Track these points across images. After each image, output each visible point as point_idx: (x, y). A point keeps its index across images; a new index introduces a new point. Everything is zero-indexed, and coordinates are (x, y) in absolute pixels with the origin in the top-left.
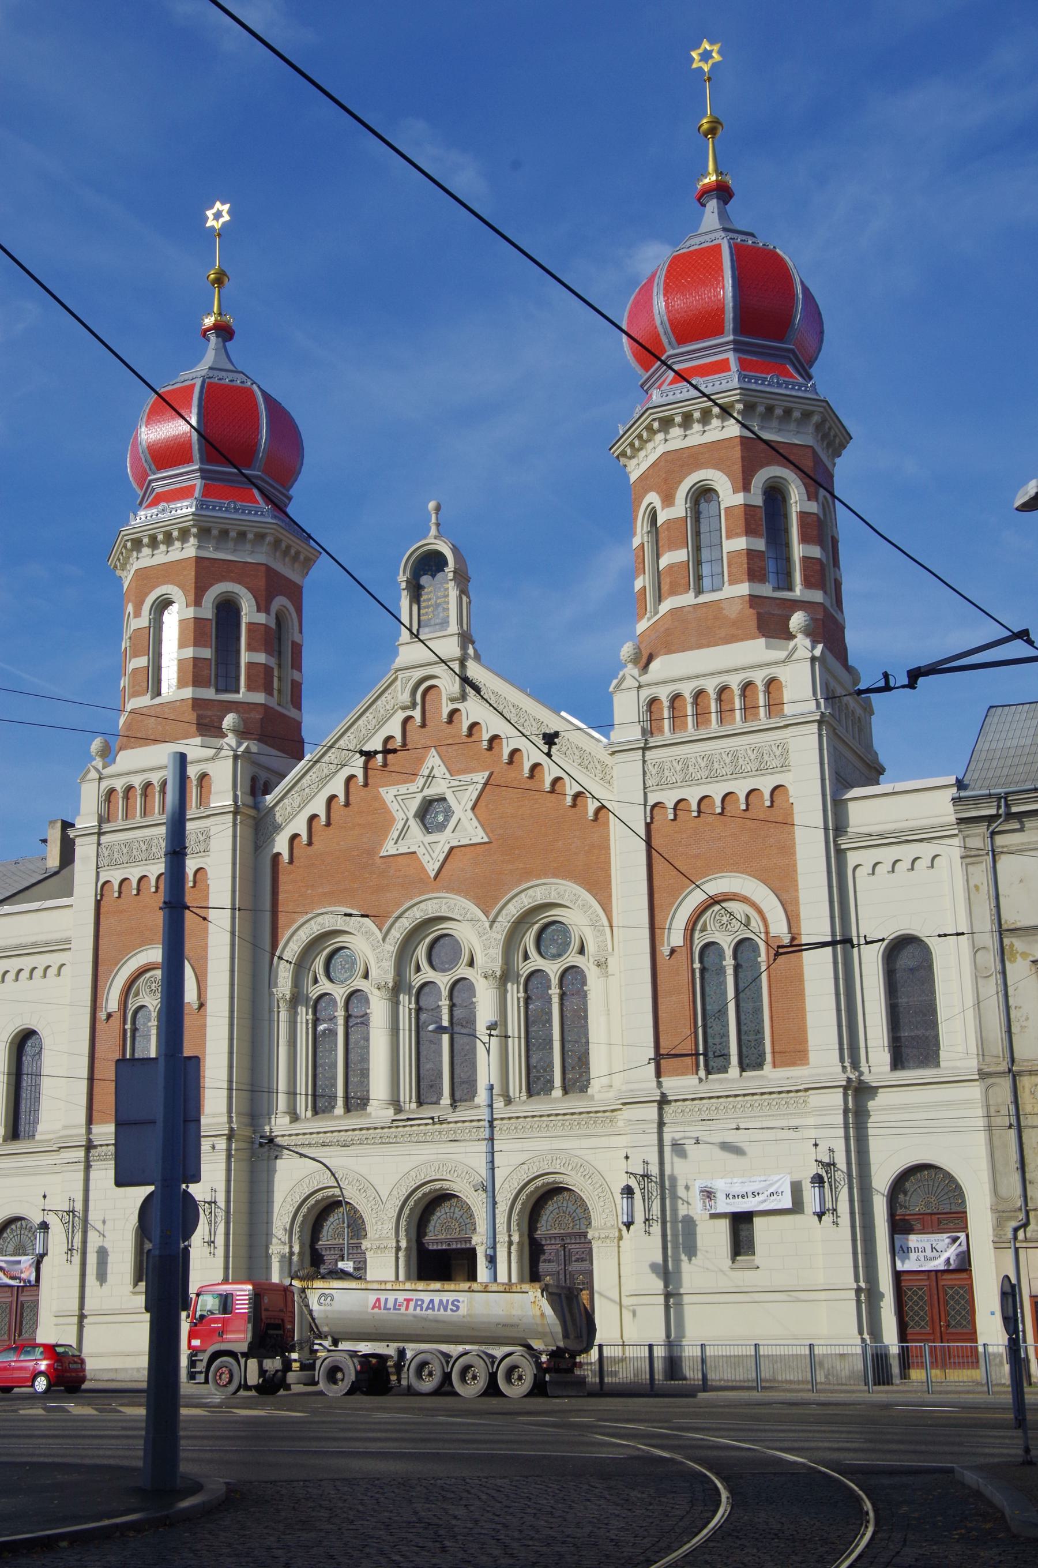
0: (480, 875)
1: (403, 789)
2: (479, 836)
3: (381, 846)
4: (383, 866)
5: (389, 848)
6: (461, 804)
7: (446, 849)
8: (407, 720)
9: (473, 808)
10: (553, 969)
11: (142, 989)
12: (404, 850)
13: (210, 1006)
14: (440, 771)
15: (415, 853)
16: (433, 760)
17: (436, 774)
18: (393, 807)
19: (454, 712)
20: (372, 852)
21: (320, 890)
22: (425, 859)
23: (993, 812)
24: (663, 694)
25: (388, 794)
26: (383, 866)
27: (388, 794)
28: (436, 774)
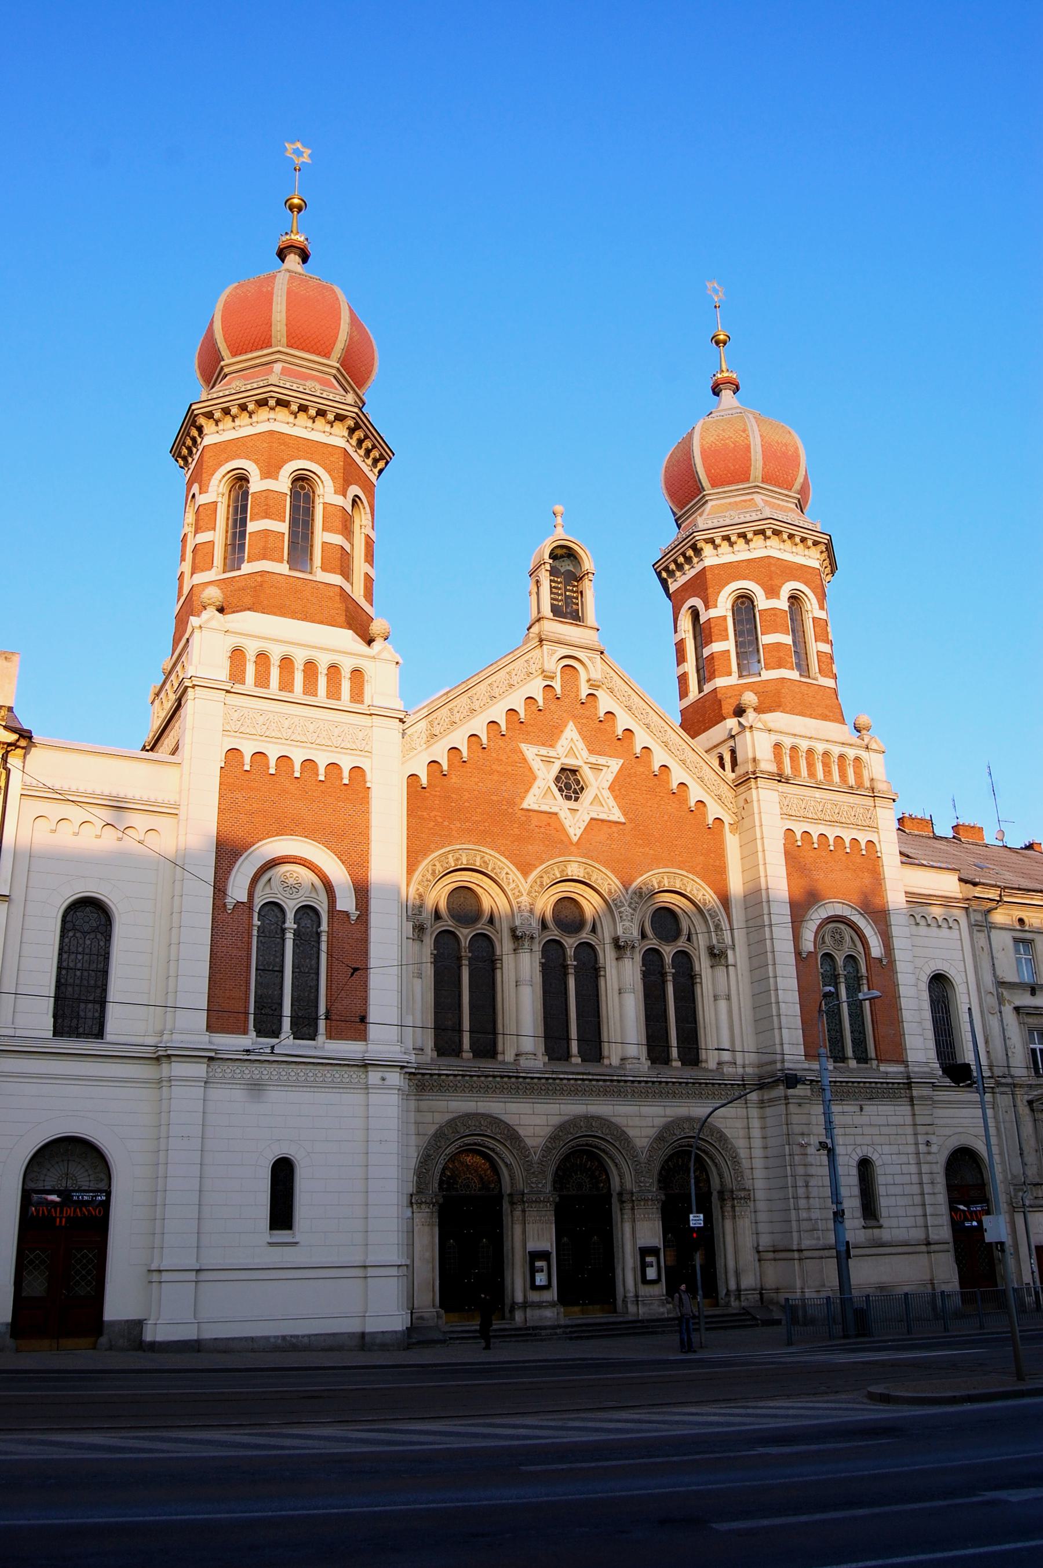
1: (544, 751)
2: (617, 815)
3: (523, 799)
4: (524, 818)
5: (531, 801)
6: (599, 783)
7: (587, 819)
10: (668, 951)
12: (545, 808)
13: (374, 919)
14: (581, 744)
15: (556, 814)
16: (571, 733)
17: (571, 746)
18: (536, 764)
20: (512, 803)
22: (567, 823)
24: (788, 742)
25: (530, 752)
26: (524, 818)
27: (530, 752)
28: (571, 746)
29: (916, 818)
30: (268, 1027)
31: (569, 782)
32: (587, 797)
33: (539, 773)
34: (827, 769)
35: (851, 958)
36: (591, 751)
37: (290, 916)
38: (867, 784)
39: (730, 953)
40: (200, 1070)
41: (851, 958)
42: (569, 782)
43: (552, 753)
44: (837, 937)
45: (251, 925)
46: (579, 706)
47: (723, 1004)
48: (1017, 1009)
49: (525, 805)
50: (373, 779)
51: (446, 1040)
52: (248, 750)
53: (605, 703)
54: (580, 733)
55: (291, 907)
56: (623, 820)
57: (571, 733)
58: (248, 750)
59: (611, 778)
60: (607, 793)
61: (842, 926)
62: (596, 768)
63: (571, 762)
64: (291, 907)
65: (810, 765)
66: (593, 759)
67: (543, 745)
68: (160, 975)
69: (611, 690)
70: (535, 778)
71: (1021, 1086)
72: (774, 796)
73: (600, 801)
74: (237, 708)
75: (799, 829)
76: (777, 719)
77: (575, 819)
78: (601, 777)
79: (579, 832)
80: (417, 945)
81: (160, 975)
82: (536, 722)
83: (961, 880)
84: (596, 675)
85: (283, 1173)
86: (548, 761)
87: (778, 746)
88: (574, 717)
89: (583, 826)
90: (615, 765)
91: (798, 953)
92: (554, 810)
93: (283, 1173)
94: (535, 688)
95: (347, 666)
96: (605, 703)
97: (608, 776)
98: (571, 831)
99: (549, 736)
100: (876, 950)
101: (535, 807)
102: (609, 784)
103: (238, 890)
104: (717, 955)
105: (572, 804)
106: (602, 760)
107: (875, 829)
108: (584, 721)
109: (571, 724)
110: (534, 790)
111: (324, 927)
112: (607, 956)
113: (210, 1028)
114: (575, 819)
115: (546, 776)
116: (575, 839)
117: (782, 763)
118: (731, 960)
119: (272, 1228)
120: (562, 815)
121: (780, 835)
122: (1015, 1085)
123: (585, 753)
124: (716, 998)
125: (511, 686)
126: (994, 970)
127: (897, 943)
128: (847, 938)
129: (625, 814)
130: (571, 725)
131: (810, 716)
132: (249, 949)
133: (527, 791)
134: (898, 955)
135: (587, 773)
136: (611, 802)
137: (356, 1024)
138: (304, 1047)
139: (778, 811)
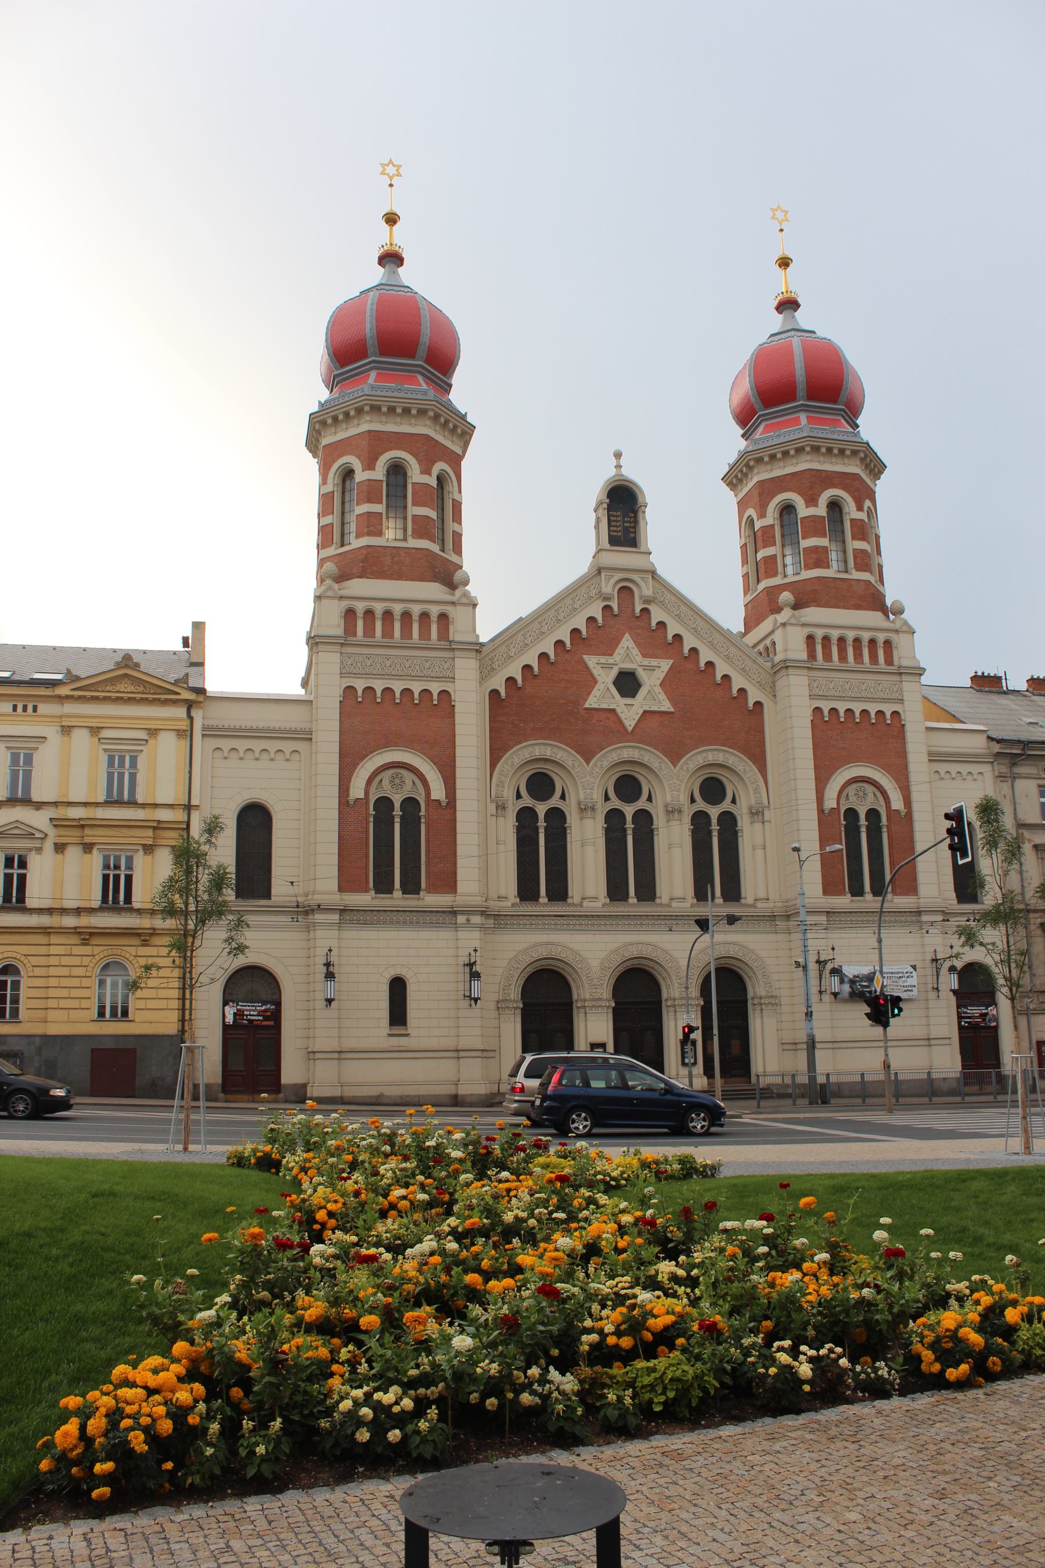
0: (670, 735)
1: (603, 659)
2: (666, 706)
5: (592, 701)
7: (641, 712)
8: (607, 608)
10: (714, 812)
11: (386, 784)
12: (605, 706)
14: (635, 651)
15: (613, 711)
16: (627, 642)
17: (627, 653)
18: (596, 671)
19: (645, 611)
21: (532, 725)
23: (1019, 752)
28: (627, 653)
29: (989, 676)
30: (383, 886)
31: (627, 683)
32: (642, 693)
34: (858, 652)
35: (873, 814)
36: (644, 656)
37: (397, 805)
38: (896, 661)
39: (766, 812)
40: (336, 917)
41: (873, 814)
42: (627, 683)
44: (861, 793)
45: (368, 814)
47: (759, 853)
48: (1036, 847)
49: (587, 705)
50: (458, 698)
51: (527, 891)
52: (360, 685)
53: (657, 615)
54: (635, 642)
55: (397, 800)
57: (627, 642)
58: (360, 685)
59: (662, 677)
61: (866, 785)
62: (647, 668)
63: (628, 666)
64: (397, 800)
65: (842, 651)
67: (603, 655)
68: (307, 854)
70: (596, 682)
71: (1035, 911)
72: (805, 680)
73: (654, 695)
74: (349, 655)
75: (826, 706)
76: (814, 614)
77: (629, 712)
78: (653, 675)
79: (633, 723)
80: (501, 819)
81: (307, 854)
82: (597, 636)
83: (989, 737)
85: (398, 988)
86: (607, 667)
87: (810, 639)
88: (630, 630)
89: (637, 717)
90: (665, 665)
91: (820, 810)
92: (612, 707)
93: (398, 988)
95: (434, 611)
96: (657, 615)
97: (660, 675)
100: (897, 803)
101: (596, 706)
102: (659, 682)
103: (357, 791)
104: (757, 814)
105: (629, 701)
106: (654, 662)
107: (901, 701)
108: (639, 631)
109: (627, 636)
110: (595, 692)
111: (423, 813)
112: (659, 821)
113: (341, 889)
114: (629, 712)
115: (605, 679)
116: (630, 729)
117: (815, 651)
118: (766, 818)
119: (391, 1025)
120: (619, 710)
121: (808, 714)
122: (1028, 911)
123: (639, 658)
124: (754, 848)
126: (1015, 814)
127: (914, 797)
128: (870, 796)
129: (674, 704)
130: (627, 636)
131: (844, 608)
132: (367, 832)
133: (589, 694)
134: (915, 806)
135: (642, 675)
136: (662, 696)
137: (448, 882)
138: (411, 902)
139: (806, 692)
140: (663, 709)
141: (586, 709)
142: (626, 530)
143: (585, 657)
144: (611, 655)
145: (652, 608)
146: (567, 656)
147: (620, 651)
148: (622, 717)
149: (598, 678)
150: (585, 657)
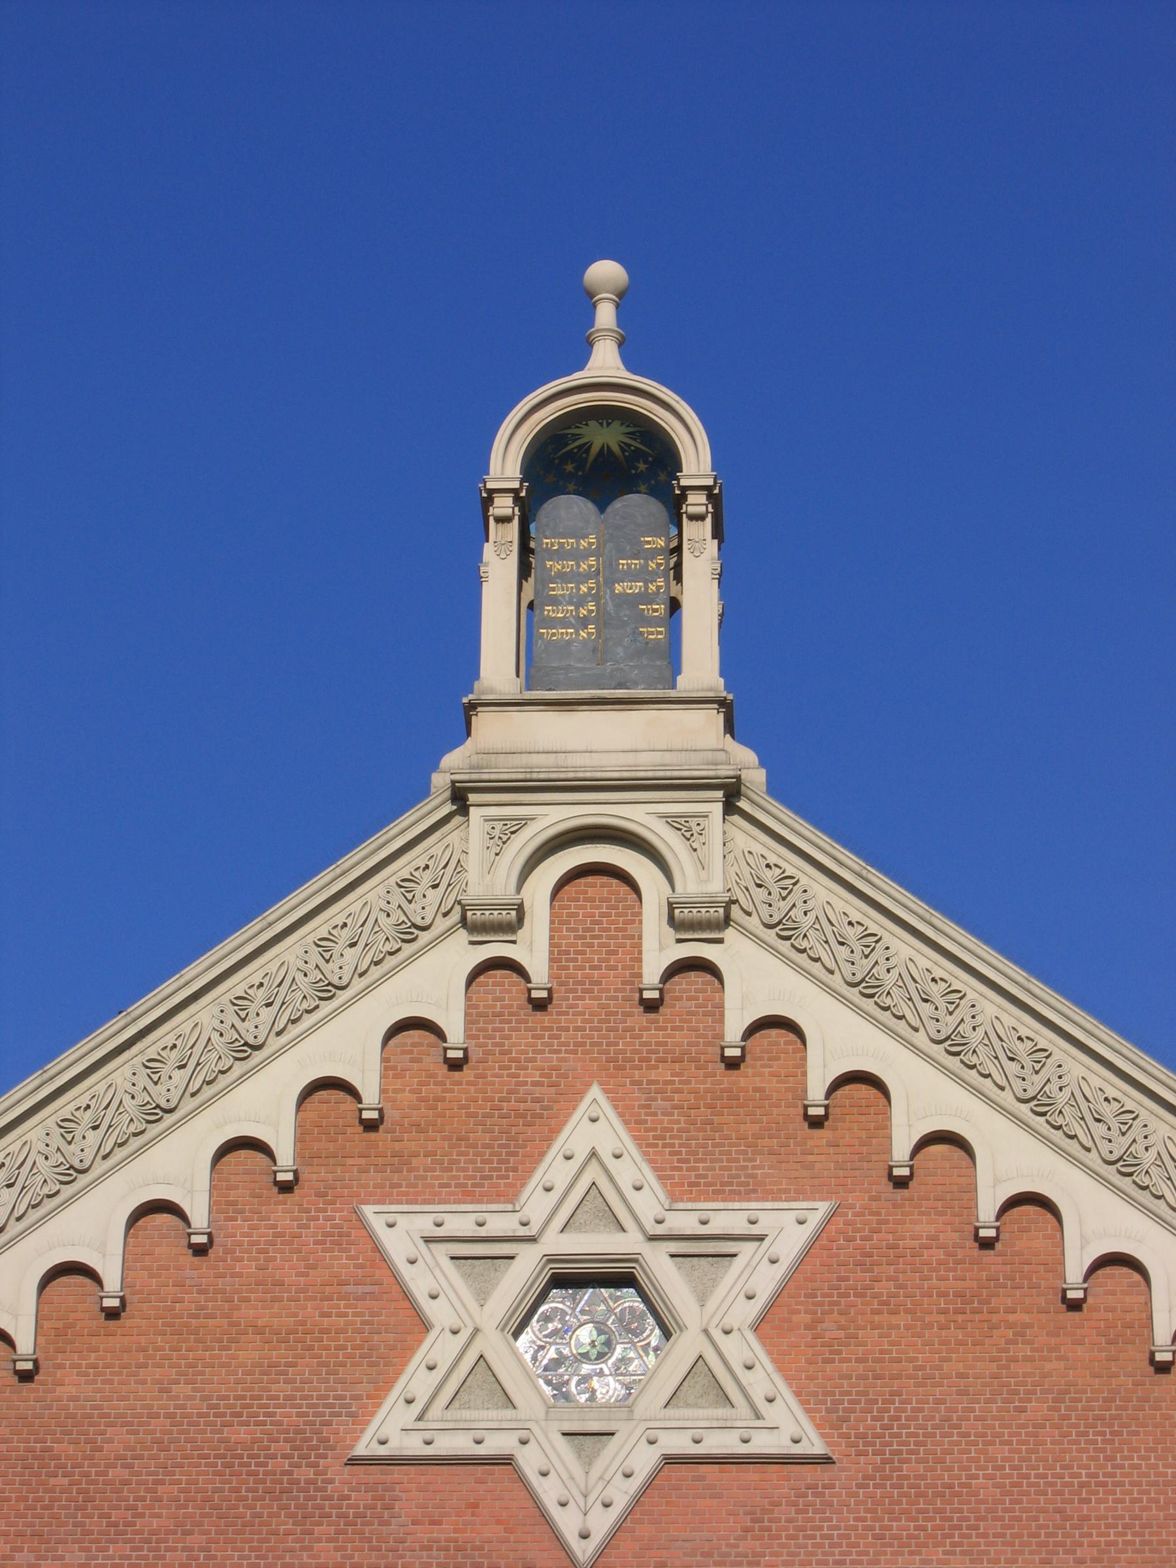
2: (787, 1427)
3: (360, 1420)
5: (391, 1428)
7: (645, 1461)
9: (757, 1327)
15: (506, 1461)
16: (594, 1129)
18: (429, 1278)
33: (438, 1313)
36: (683, 1185)
43: (500, 1223)
46: (640, 1018)
56: (814, 1445)
57: (594, 1129)
60: (742, 1348)
66: (685, 1222)
69: (784, 929)
79: (602, 1523)
84: (702, 877)
86: (481, 1256)
88: (615, 1070)
92: (495, 1445)
94: (436, 981)
98: (568, 1523)
99: (501, 1153)
101: (413, 1446)
106: (728, 1218)
109: (595, 1092)
110: (416, 1380)
120: (529, 1461)
123: (649, 1203)
125: (328, 990)
130: (595, 1092)
136: (764, 1379)
140: (763, 1444)
141: (354, 1462)
142: (615, 618)
143: (368, 1210)
144: (507, 1193)
145: (732, 953)
146: (283, 1213)
147: (554, 1170)
148: (548, 1492)
149: (431, 1309)
150: (368, 1210)
